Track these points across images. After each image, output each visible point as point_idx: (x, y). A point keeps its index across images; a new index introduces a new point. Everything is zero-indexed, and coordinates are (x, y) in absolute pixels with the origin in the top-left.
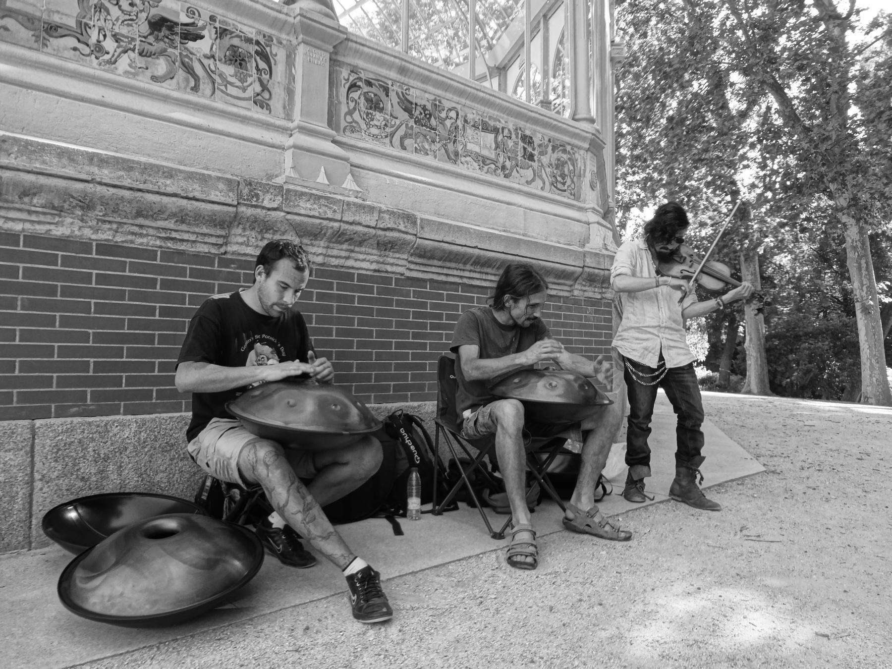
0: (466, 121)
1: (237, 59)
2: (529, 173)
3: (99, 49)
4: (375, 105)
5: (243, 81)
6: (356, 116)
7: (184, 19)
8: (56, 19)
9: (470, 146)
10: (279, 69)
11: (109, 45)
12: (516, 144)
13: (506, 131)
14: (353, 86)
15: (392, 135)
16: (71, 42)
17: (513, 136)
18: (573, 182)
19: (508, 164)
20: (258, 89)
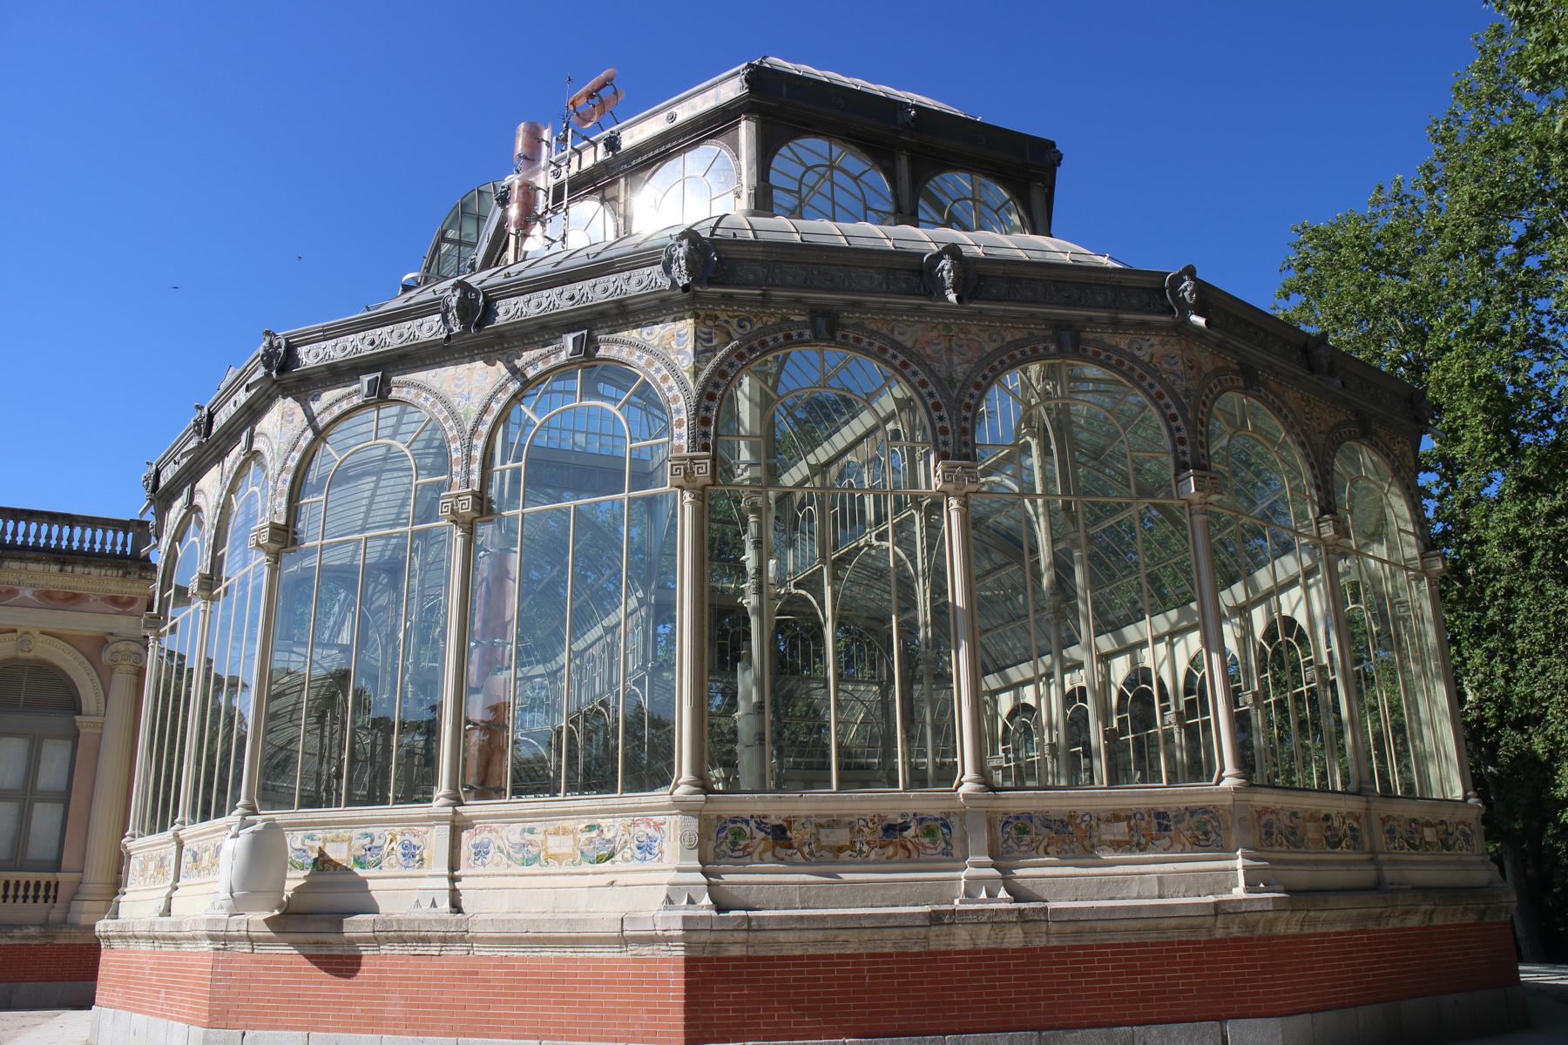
0: (1099, 819)
1: (930, 833)
2: (1167, 842)
3: (861, 852)
4: (1023, 831)
5: (935, 843)
6: (1010, 842)
7: (900, 821)
8: (842, 843)
9: (1104, 837)
10: (956, 832)
11: (865, 848)
12: (1149, 823)
13: (1138, 816)
14: (1007, 823)
15: (1037, 847)
16: (849, 852)
17: (1146, 817)
18: (1218, 835)
19: (1143, 840)
20: (944, 845)
